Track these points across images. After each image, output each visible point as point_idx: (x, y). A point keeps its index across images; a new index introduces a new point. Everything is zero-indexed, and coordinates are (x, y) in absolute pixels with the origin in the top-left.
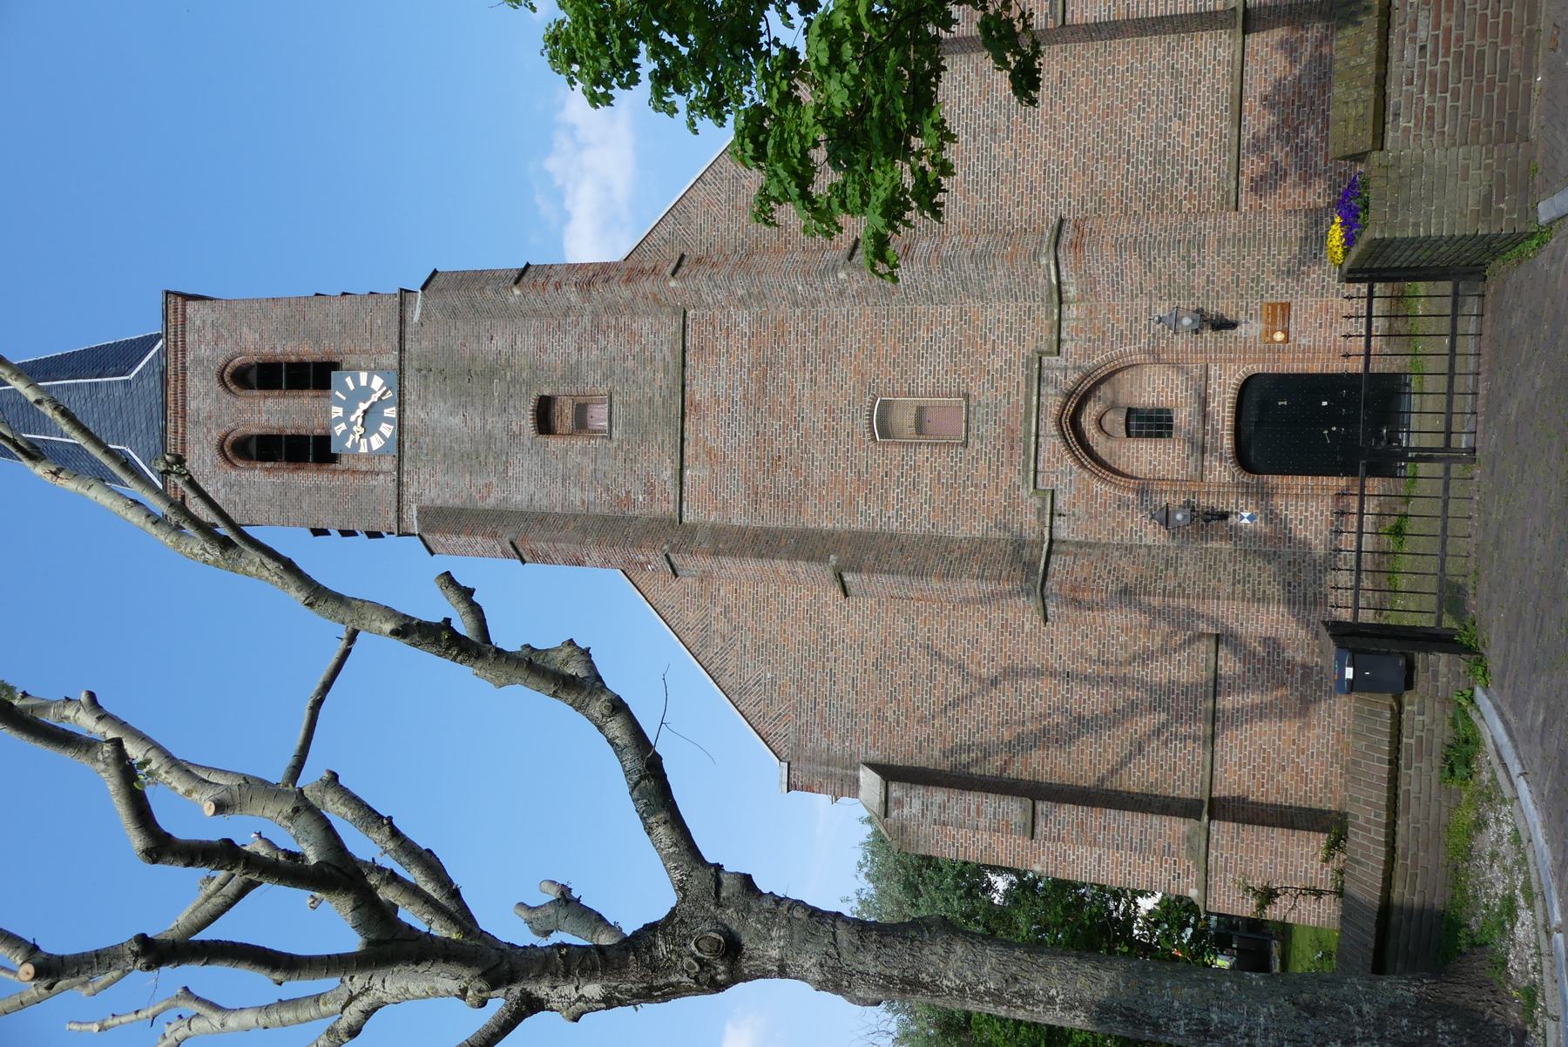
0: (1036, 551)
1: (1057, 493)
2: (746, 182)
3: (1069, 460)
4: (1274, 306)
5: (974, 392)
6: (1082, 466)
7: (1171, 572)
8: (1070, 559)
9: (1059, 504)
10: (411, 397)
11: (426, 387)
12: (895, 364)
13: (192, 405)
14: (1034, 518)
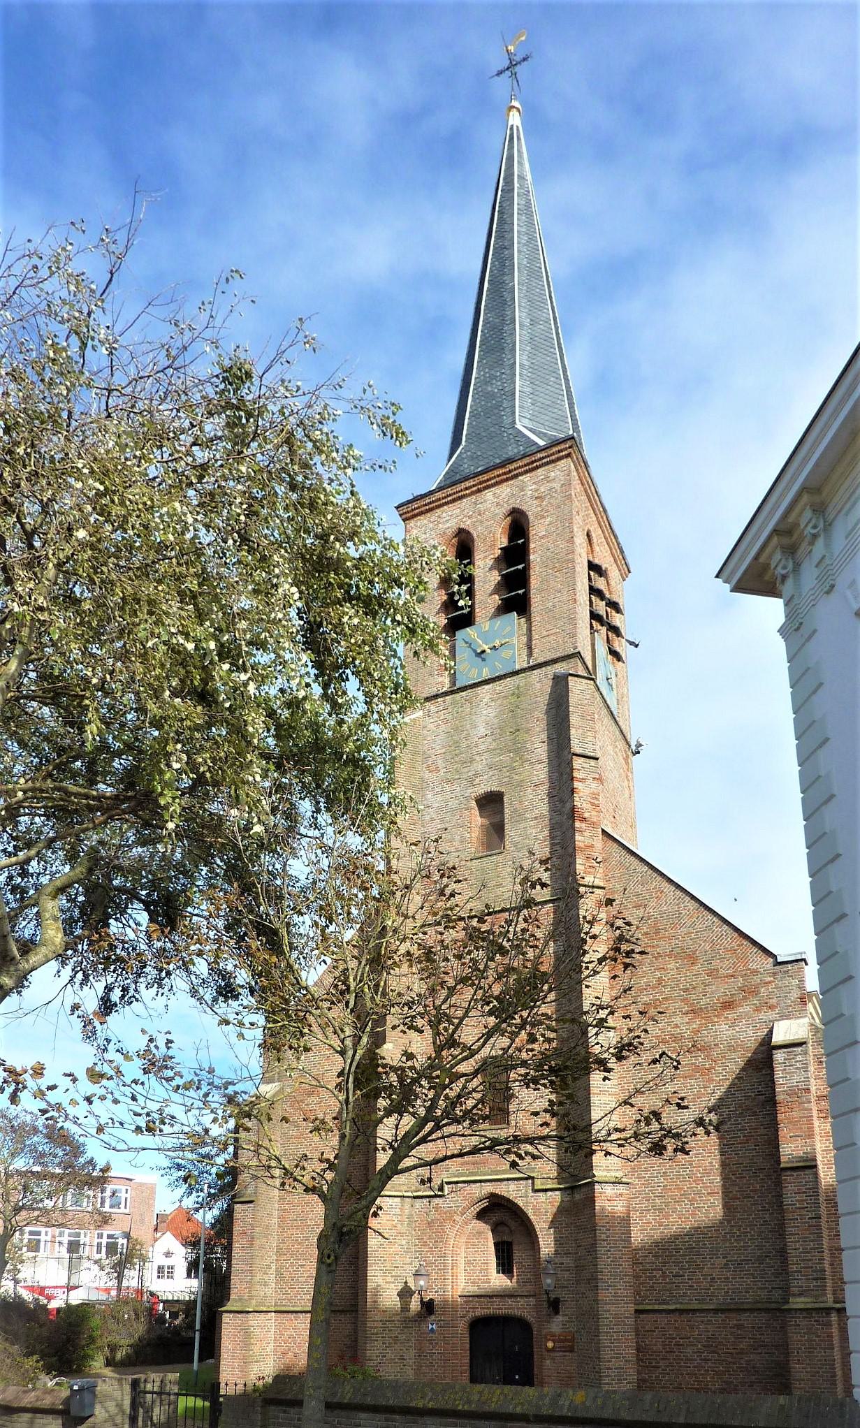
4: (573, 1340)
9: (437, 1200)
13: (489, 495)
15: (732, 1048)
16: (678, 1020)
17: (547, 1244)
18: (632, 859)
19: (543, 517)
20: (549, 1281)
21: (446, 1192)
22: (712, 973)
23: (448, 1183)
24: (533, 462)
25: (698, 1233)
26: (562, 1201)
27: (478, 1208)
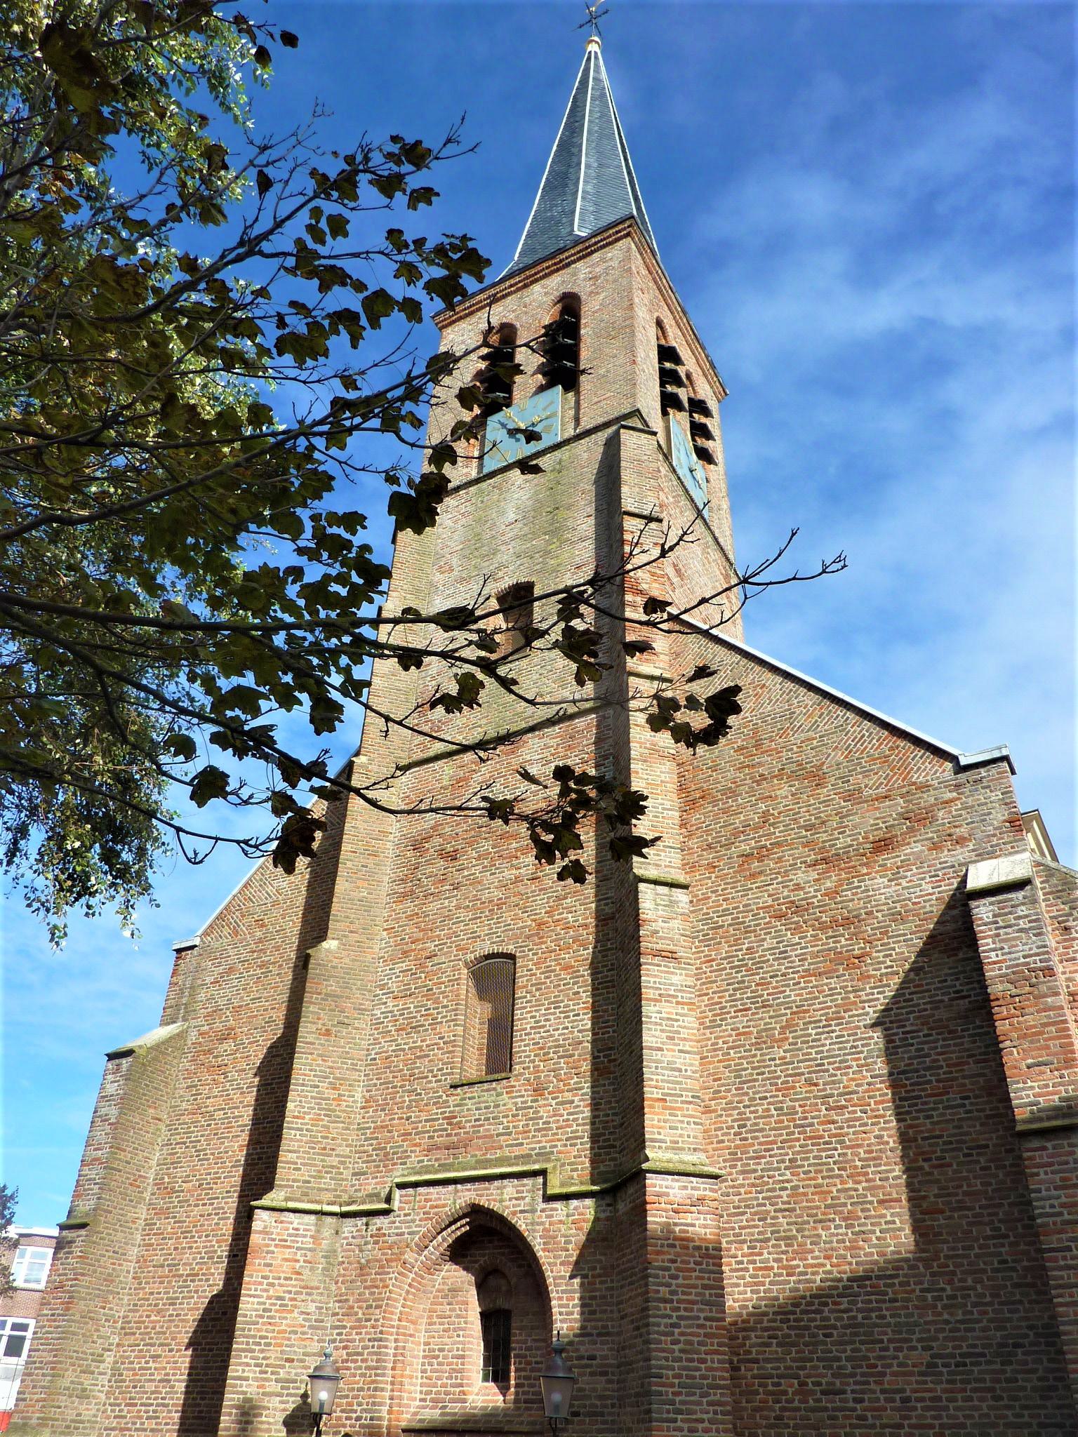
1: (391, 1217)
7: (273, 1387)
9: (379, 1221)
13: (537, 288)
14: (370, 1189)
15: (897, 917)
16: (800, 876)
17: (566, 1311)
18: (718, 648)
19: (598, 293)
20: (557, 1397)
21: (396, 1204)
22: (852, 796)
23: (401, 1186)
24: (587, 248)
25: (865, 1285)
26: (596, 1220)
27: (449, 1236)
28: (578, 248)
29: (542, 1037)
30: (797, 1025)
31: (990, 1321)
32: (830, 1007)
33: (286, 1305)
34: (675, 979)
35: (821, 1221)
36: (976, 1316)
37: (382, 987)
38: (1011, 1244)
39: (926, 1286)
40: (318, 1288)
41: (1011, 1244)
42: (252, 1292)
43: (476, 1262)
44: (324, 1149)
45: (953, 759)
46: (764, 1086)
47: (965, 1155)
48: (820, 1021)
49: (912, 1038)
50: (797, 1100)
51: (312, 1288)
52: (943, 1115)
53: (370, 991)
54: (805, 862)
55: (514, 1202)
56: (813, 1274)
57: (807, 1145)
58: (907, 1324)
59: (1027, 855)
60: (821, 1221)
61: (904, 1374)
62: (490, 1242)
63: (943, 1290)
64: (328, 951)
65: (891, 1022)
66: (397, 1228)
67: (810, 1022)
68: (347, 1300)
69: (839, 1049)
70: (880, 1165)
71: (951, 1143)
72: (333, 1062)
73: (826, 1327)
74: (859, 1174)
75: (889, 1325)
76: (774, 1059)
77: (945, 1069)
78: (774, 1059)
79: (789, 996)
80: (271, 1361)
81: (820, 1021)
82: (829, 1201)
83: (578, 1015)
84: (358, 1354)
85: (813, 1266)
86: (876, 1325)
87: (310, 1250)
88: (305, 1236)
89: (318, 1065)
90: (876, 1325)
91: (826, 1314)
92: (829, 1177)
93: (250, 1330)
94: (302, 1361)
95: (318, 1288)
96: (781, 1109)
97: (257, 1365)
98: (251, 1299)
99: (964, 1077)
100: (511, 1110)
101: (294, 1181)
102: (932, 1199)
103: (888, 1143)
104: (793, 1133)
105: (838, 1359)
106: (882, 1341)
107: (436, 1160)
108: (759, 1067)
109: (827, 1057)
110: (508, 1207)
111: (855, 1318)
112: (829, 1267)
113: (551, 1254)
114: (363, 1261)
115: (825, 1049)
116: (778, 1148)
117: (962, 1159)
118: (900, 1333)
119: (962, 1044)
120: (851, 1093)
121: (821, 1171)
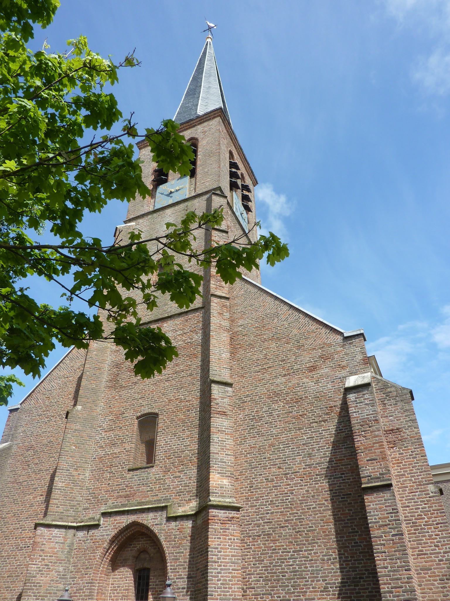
0: (71, 519)
2: (275, 321)
3: (113, 533)
5: (153, 470)
6: (112, 542)
8: (61, 540)
10: (177, 208)
11: (180, 211)
12: (172, 420)
14: (91, 516)
28: (198, 120)
29: (168, 449)
30: (275, 444)
31: (350, 568)
32: (289, 436)
33: (50, 568)
34: (225, 424)
35: (282, 527)
36: (344, 566)
37: (100, 427)
38: (360, 535)
39: (324, 554)
40: (64, 560)
41: (360, 535)
42: (34, 563)
43: (136, 547)
44: (71, 498)
45: (341, 334)
46: (260, 469)
47: (342, 498)
48: (285, 442)
49: (322, 449)
50: (274, 475)
51: (62, 560)
52: (334, 481)
53: (95, 428)
54: (281, 375)
55: (153, 520)
56: (279, 549)
57: (278, 495)
58: (317, 570)
59: (369, 373)
60: (282, 527)
61: (315, 592)
62: (142, 538)
63: (332, 555)
64: (77, 411)
65: (314, 442)
66: (101, 533)
67: (281, 443)
68: (77, 565)
69: (292, 454)
70: (307, 503)
71: (336, 493)
72: (76, 459)
73: (283, 573)
74: (298, 507)
75: (309, 571)
76: (265, 458)
77: (335, 462)
78: (265, 458)
79: (273, 431)
80: (41, 594)
81: (285, 442)
82: (286, 518)
83: (184, 439)
84: (81, 590)
85: (279, 546)
86: (304, 571)
87: (62, 543)
88: (60, 537)
89: (70, 461)
90: (304, 571)
91: (283, 567)
92: (286, 508)
93: (32, 580)
94: (56, 593)
95: (64, 560)
96: (268, 479)
97: (34, 596)
98: (34, 566)
99: (342, 465)
100: (153, 480)
101: (56, 512)
102: (328, 517)
103: (311, 493)
104: (272, 489)
105: (288, 586)
106: (306, 578)
107: (120, 502)
108: (259, 462)
109: (287, 457)
110: (150, 523)
111: (295, 568)
112: (285, 547)
113: (168, 543)
114: (86, 547)
115: (286, 454)
116: (266, 496)
117: (341, 500)
118: (313, 574)
119: (342, 451)
120: (296, 472)
121: (283, 506)
